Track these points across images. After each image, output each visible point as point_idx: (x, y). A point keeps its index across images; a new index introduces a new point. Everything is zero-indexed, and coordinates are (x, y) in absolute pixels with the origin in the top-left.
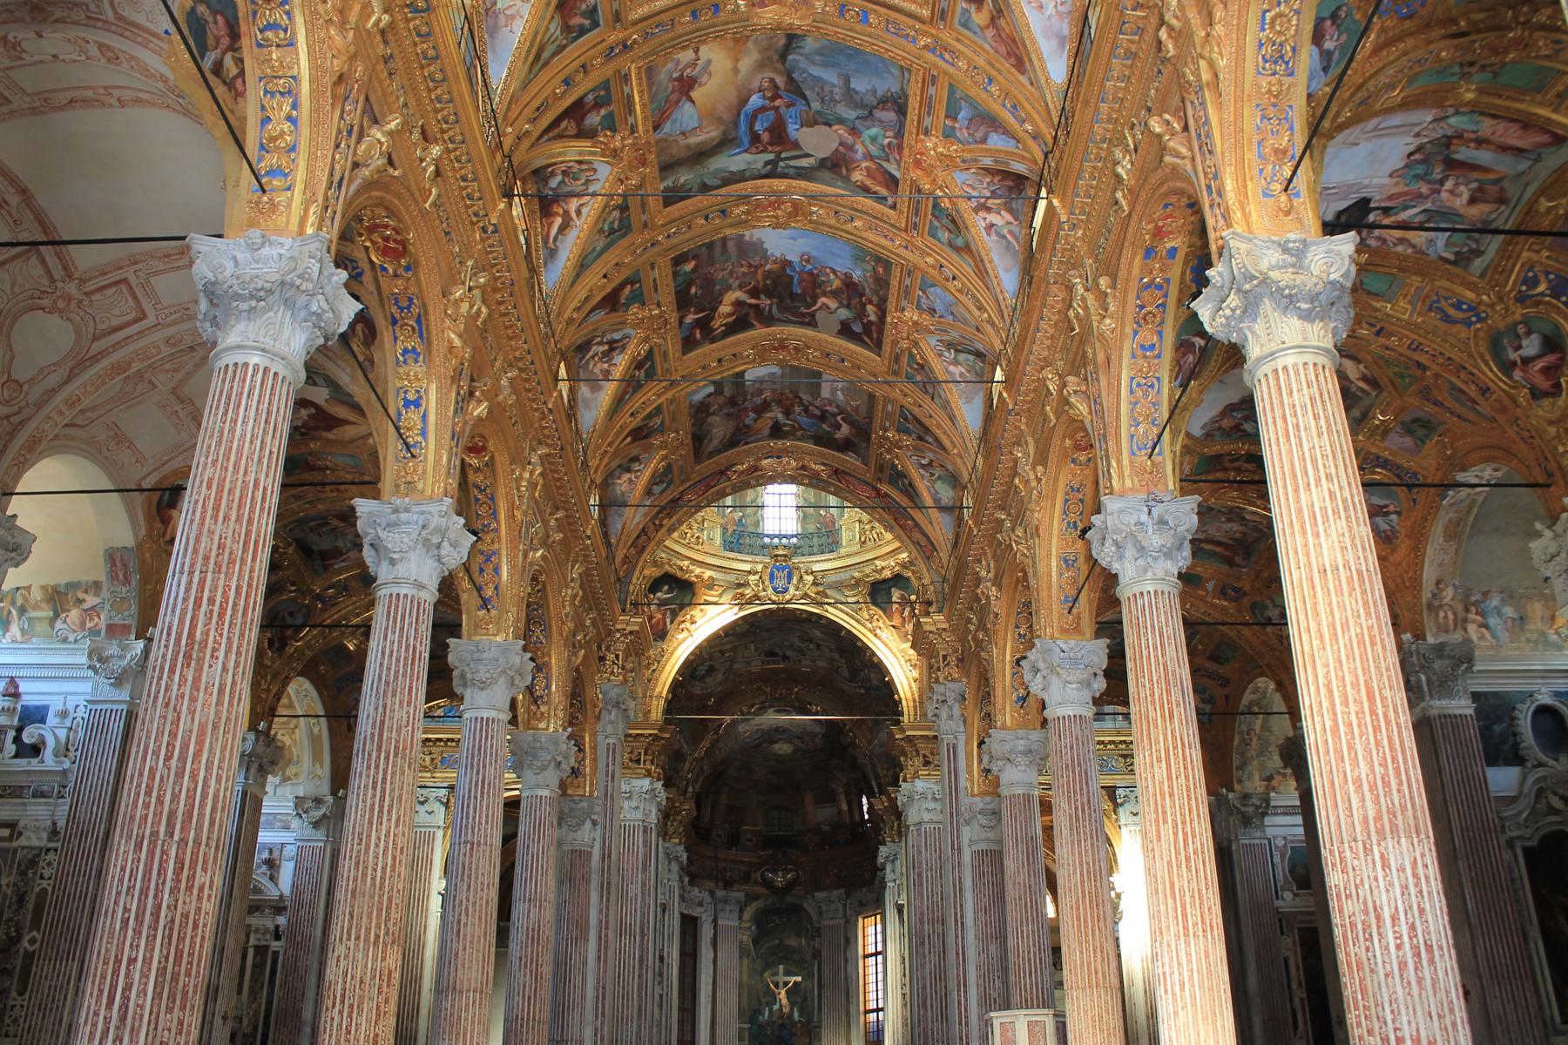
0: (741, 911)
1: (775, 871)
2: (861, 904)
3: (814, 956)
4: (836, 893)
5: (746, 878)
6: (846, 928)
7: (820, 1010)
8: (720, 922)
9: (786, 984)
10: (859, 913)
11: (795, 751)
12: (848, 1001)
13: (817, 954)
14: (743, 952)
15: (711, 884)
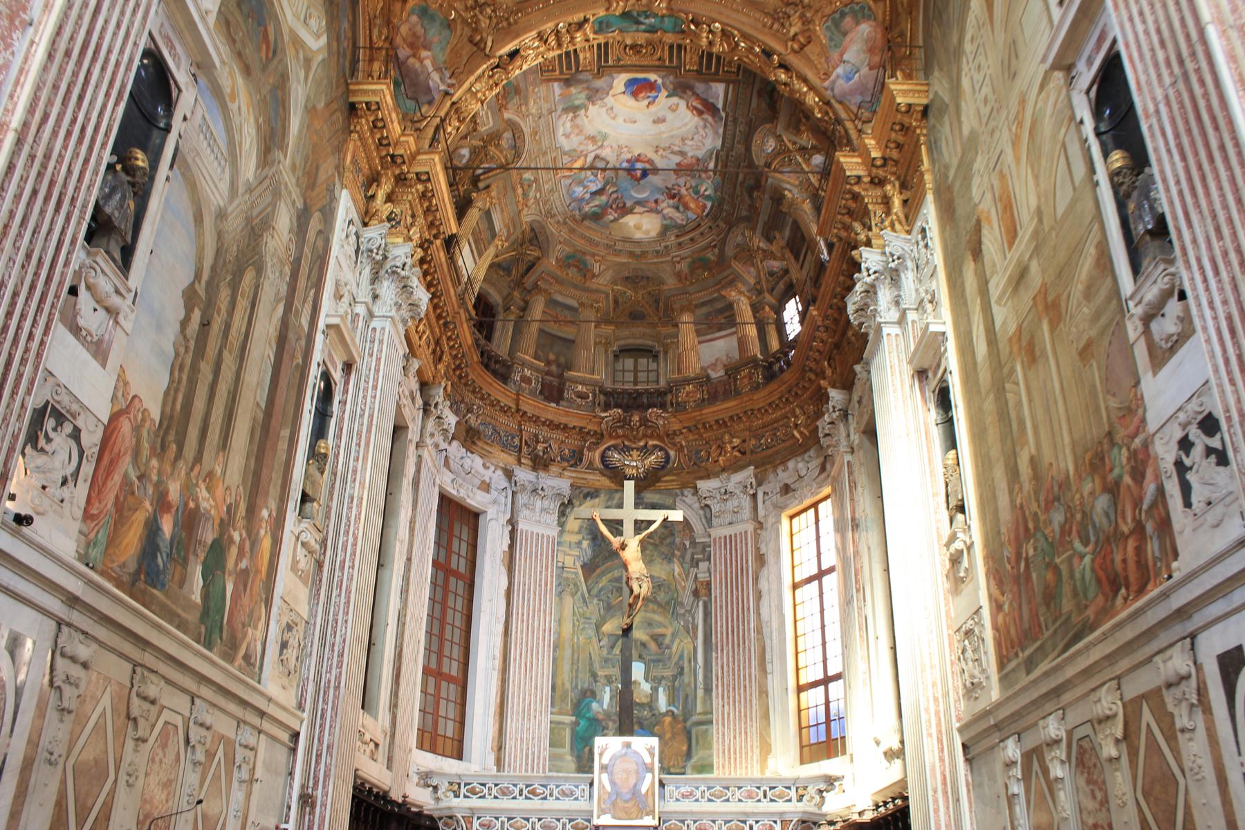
0: (562, 514)
1: (625, 450)
2: (786, 489)
3: (696, 593)
4: (738, 477)
5: (576, 458)
6: (757, 537)
7: (708, 690)
8: (522, 526)
9: (640, 526)
10: (780, 508)
11: (665, 230)
12: (763, 670)
13: (702, 591)
14: (564, 585)
15: (509, 459)
